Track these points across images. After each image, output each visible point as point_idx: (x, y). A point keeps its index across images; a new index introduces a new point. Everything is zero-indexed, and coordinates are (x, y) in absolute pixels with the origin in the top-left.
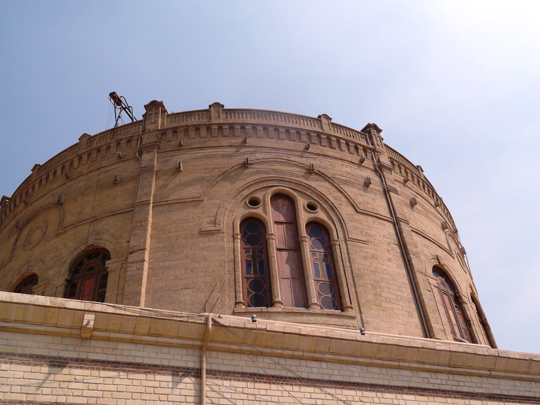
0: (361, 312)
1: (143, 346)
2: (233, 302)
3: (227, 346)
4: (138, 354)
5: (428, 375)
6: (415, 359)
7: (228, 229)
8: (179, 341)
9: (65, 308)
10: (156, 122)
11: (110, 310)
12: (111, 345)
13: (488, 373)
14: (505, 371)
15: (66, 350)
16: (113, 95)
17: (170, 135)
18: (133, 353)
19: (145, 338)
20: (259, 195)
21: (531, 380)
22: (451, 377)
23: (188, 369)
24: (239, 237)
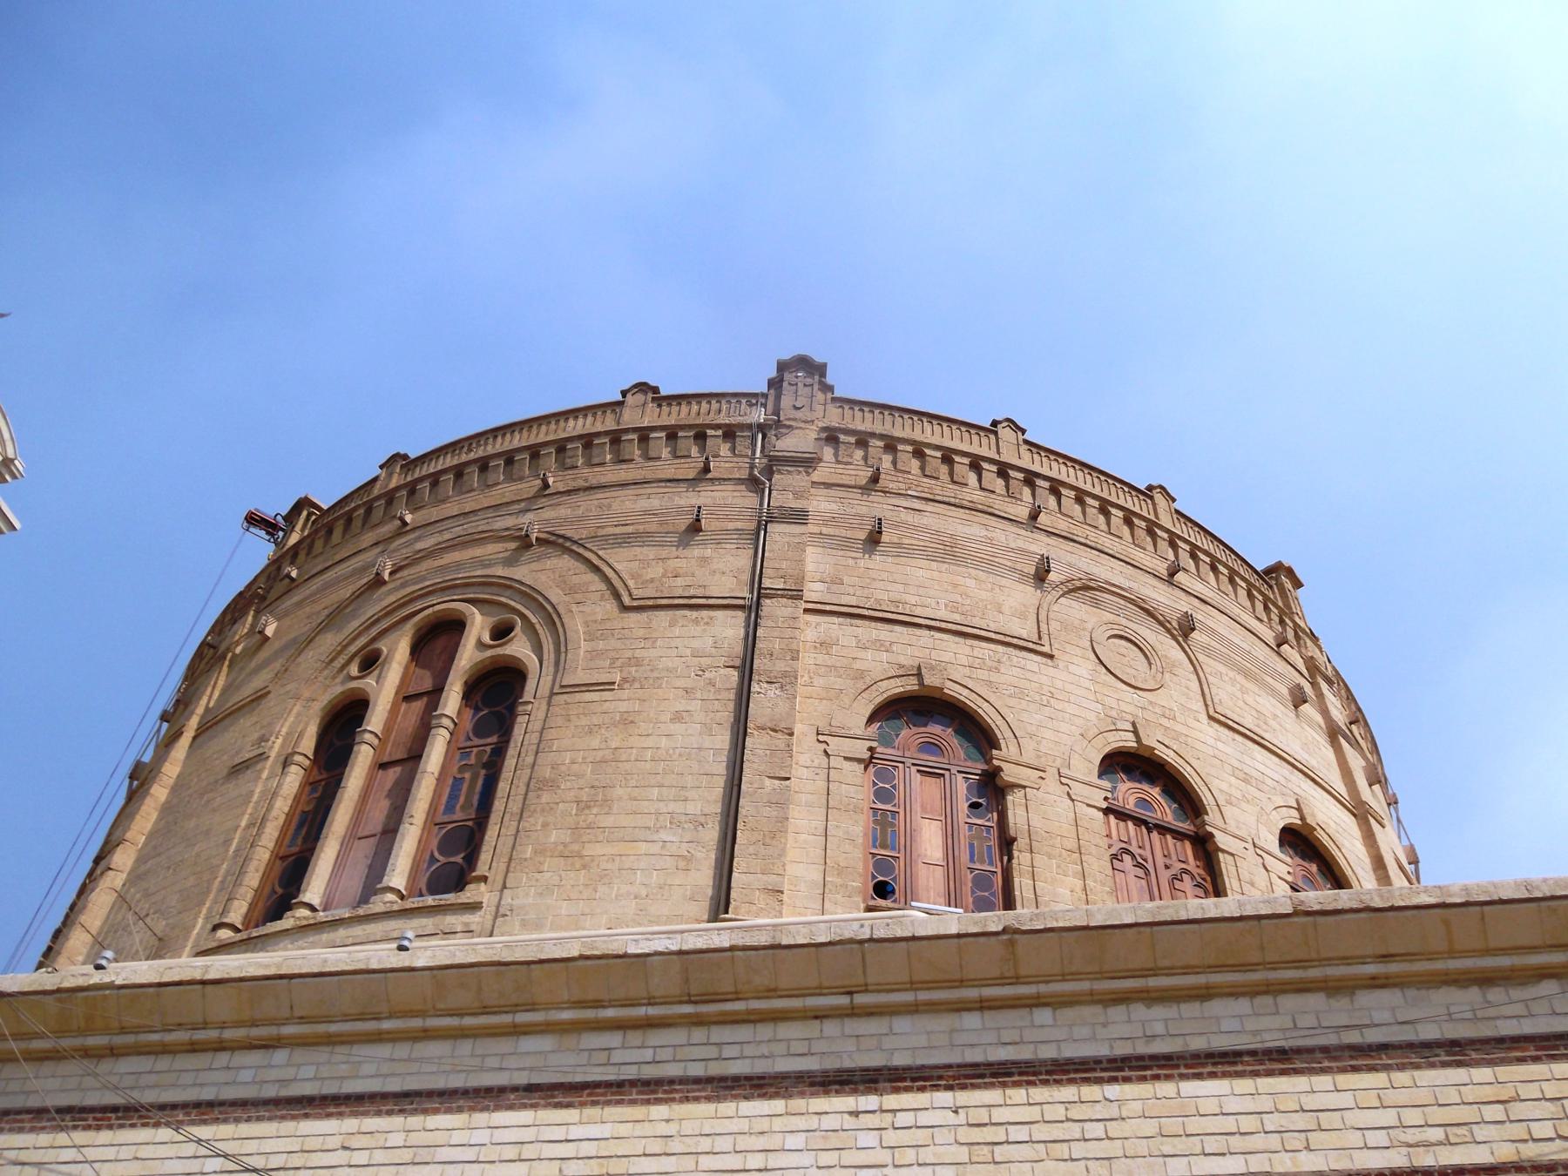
5: (614, 1039)
6: (566, 998)
13: (844, 1000)
14: (913, 986)
21: (1036, 1002)
22: (699, 1034)
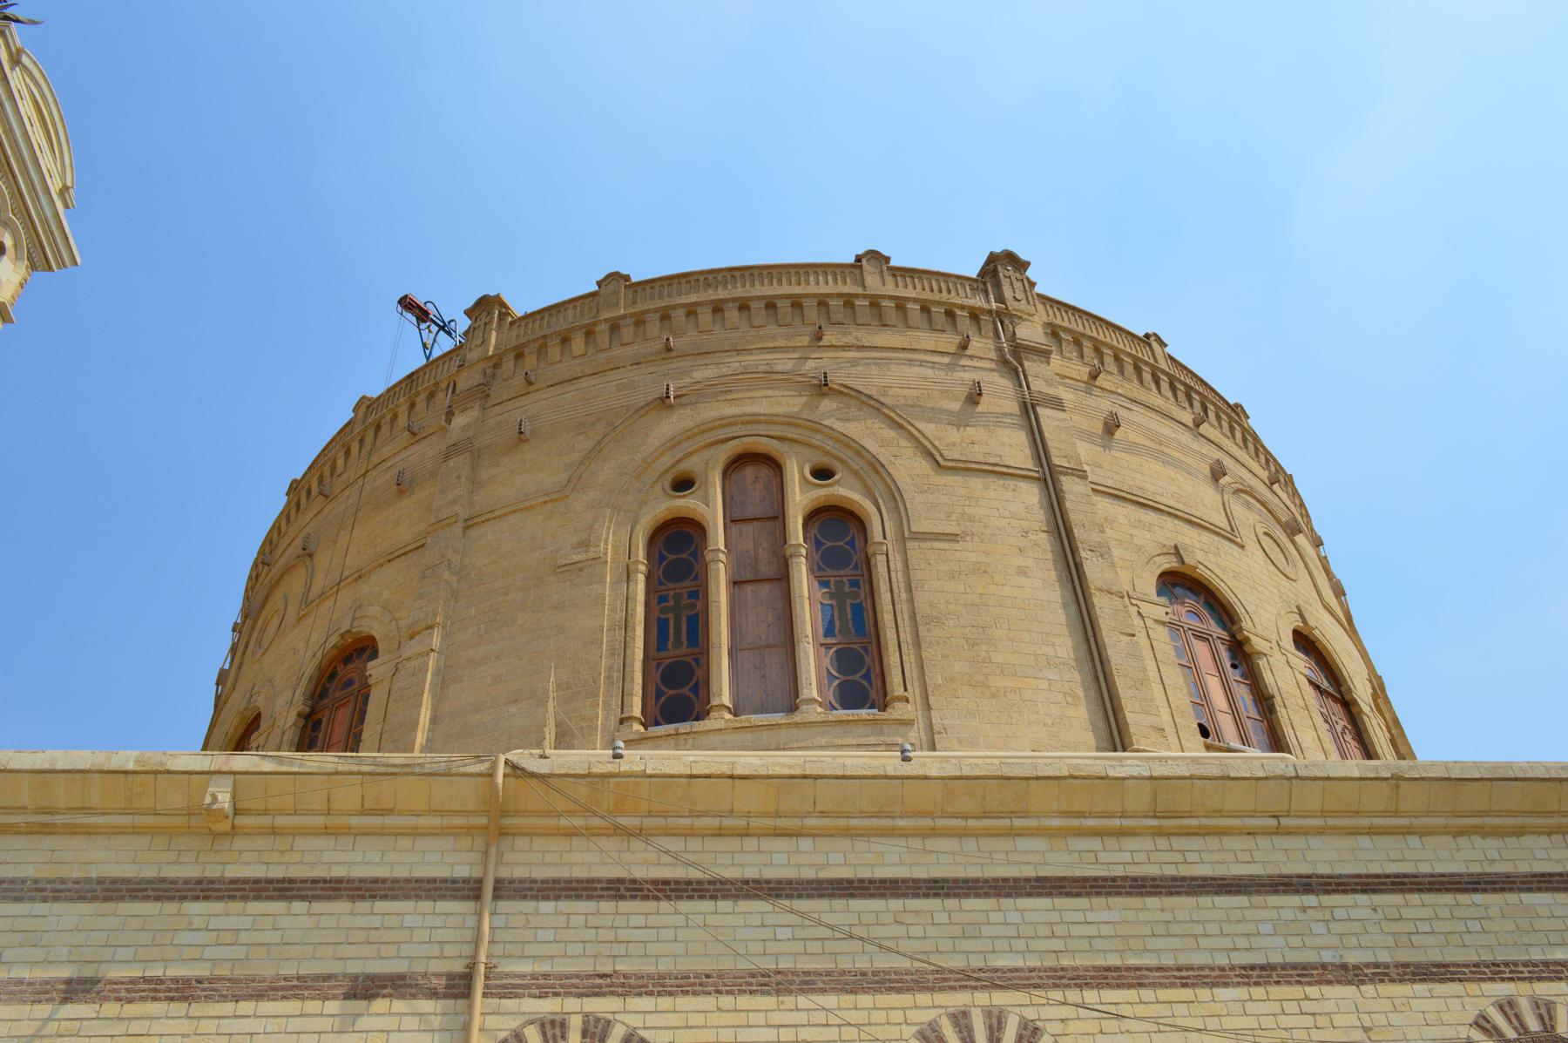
0: (928, 707)
1: (351, 839)
2: (614, 721)
3: (552, 822)
4: (340, 857)
5: (1095, 843)
6: (1055, 807)
7: (615, 552)
8: (436, 821)
9: (169, 772)
10: (484, 342)
11: (268, 766)
12: (279, 842)
13: (1274, 822)
14: (1323, 814)
15: (177, 862)
16: (407, 304)
17: (508, 364)
18: (326, 857)
19: (355, 821)
20: (693, 465)
21: (1407, 832)
22: (1162, 843)
23: (454, 881)
24: (642, 568)
